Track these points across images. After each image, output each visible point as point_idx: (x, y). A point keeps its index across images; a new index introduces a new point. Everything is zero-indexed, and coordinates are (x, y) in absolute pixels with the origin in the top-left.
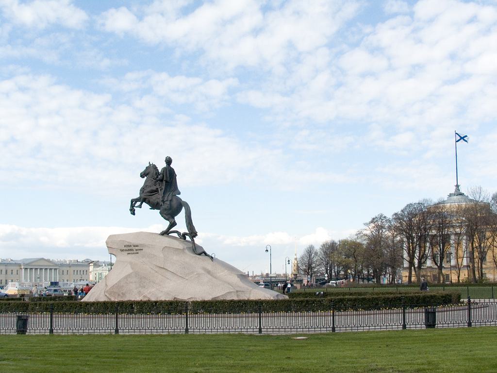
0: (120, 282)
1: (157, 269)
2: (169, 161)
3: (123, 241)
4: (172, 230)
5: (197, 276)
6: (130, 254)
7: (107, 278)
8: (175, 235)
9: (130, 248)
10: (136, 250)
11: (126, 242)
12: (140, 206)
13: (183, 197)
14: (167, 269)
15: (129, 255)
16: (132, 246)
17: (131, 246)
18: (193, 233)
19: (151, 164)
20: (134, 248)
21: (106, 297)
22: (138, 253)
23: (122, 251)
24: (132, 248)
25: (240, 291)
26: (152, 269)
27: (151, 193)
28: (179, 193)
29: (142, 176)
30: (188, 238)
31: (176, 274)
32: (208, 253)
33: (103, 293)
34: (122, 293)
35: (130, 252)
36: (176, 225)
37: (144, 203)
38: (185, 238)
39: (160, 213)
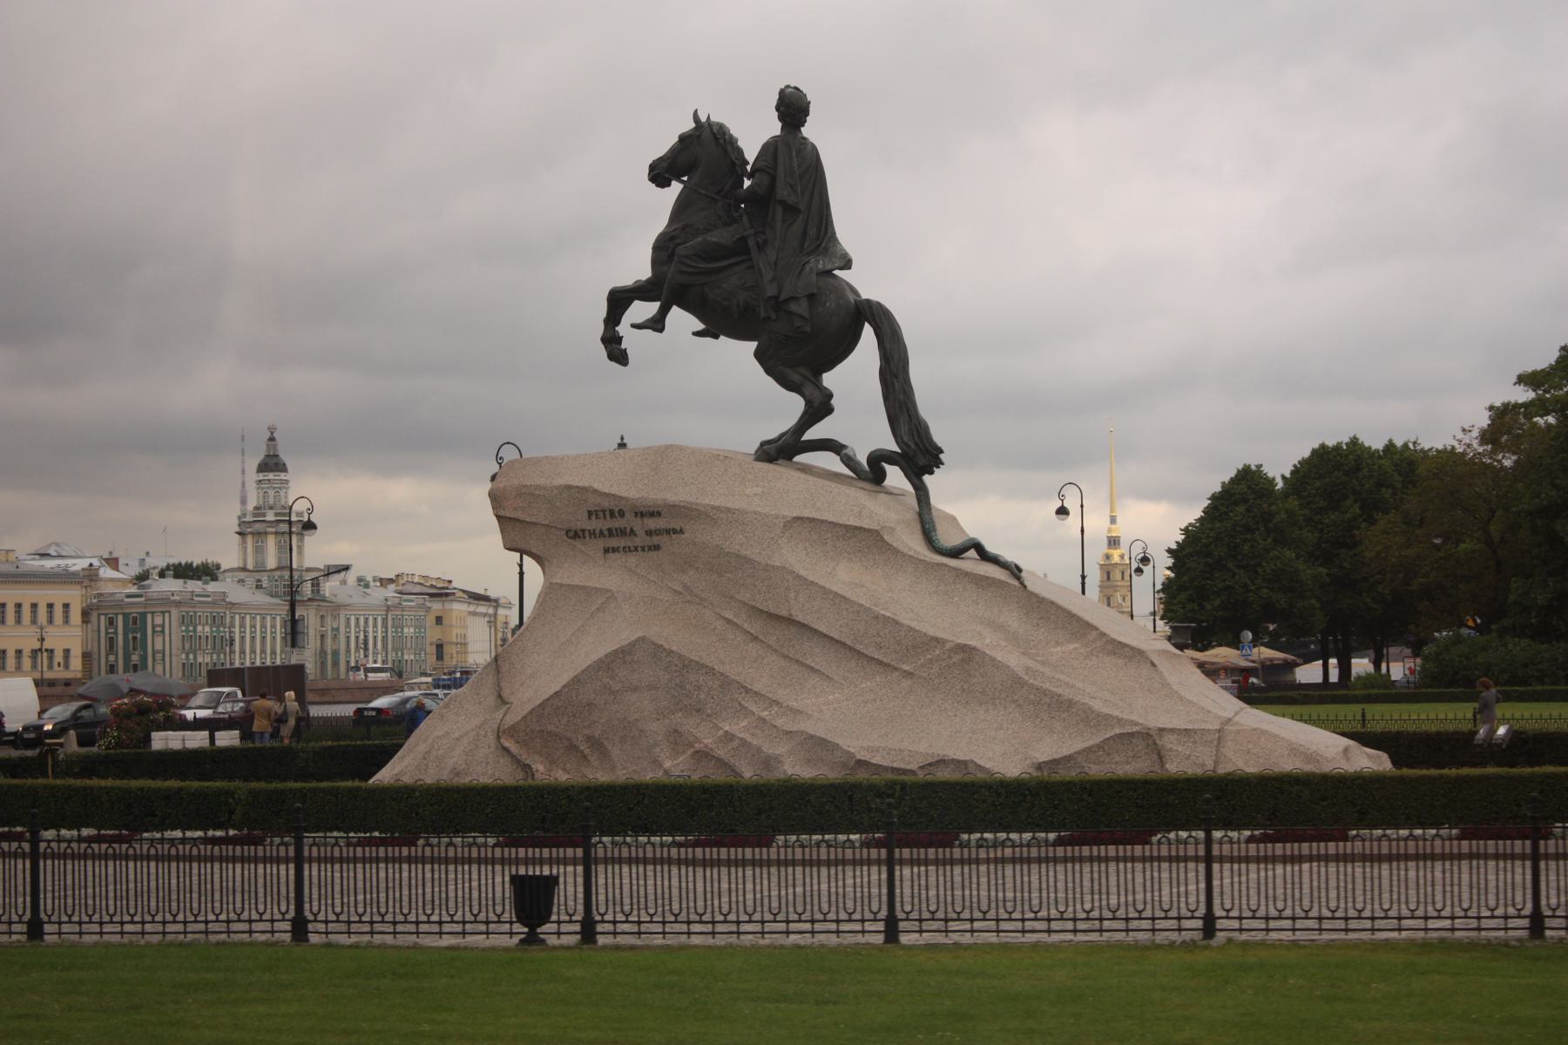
0: (576, 681)
1: (755, 627)
2: (793, 108)
4: (812, 434)
5: (956, 658)
6: (615, 550)
7: (504, 669)
8: (828, 461)
9: (618, 523)
10: (649, 533)
11: (595, 491)
12: (657, 324)
13: (866, 279)
15: (611, 555)
17: (622, 513)
18: (919, 455)
19: (703, 119)
20: (638, 525)
21: (504, 761)
22: (657, 548)
24: (629, 521)
25: (1172, 730)
26: (728, 621)
27: (715, 259)
28: (847, 264)
29: (660, 174)
30: (895, 477)
31: (851, 649)
32: (991, 548)
33: (491, 737)
34: (589, 738)
36: (830, 410)
37: (675, 308)
38: (878, 477)
39: (759, 355)
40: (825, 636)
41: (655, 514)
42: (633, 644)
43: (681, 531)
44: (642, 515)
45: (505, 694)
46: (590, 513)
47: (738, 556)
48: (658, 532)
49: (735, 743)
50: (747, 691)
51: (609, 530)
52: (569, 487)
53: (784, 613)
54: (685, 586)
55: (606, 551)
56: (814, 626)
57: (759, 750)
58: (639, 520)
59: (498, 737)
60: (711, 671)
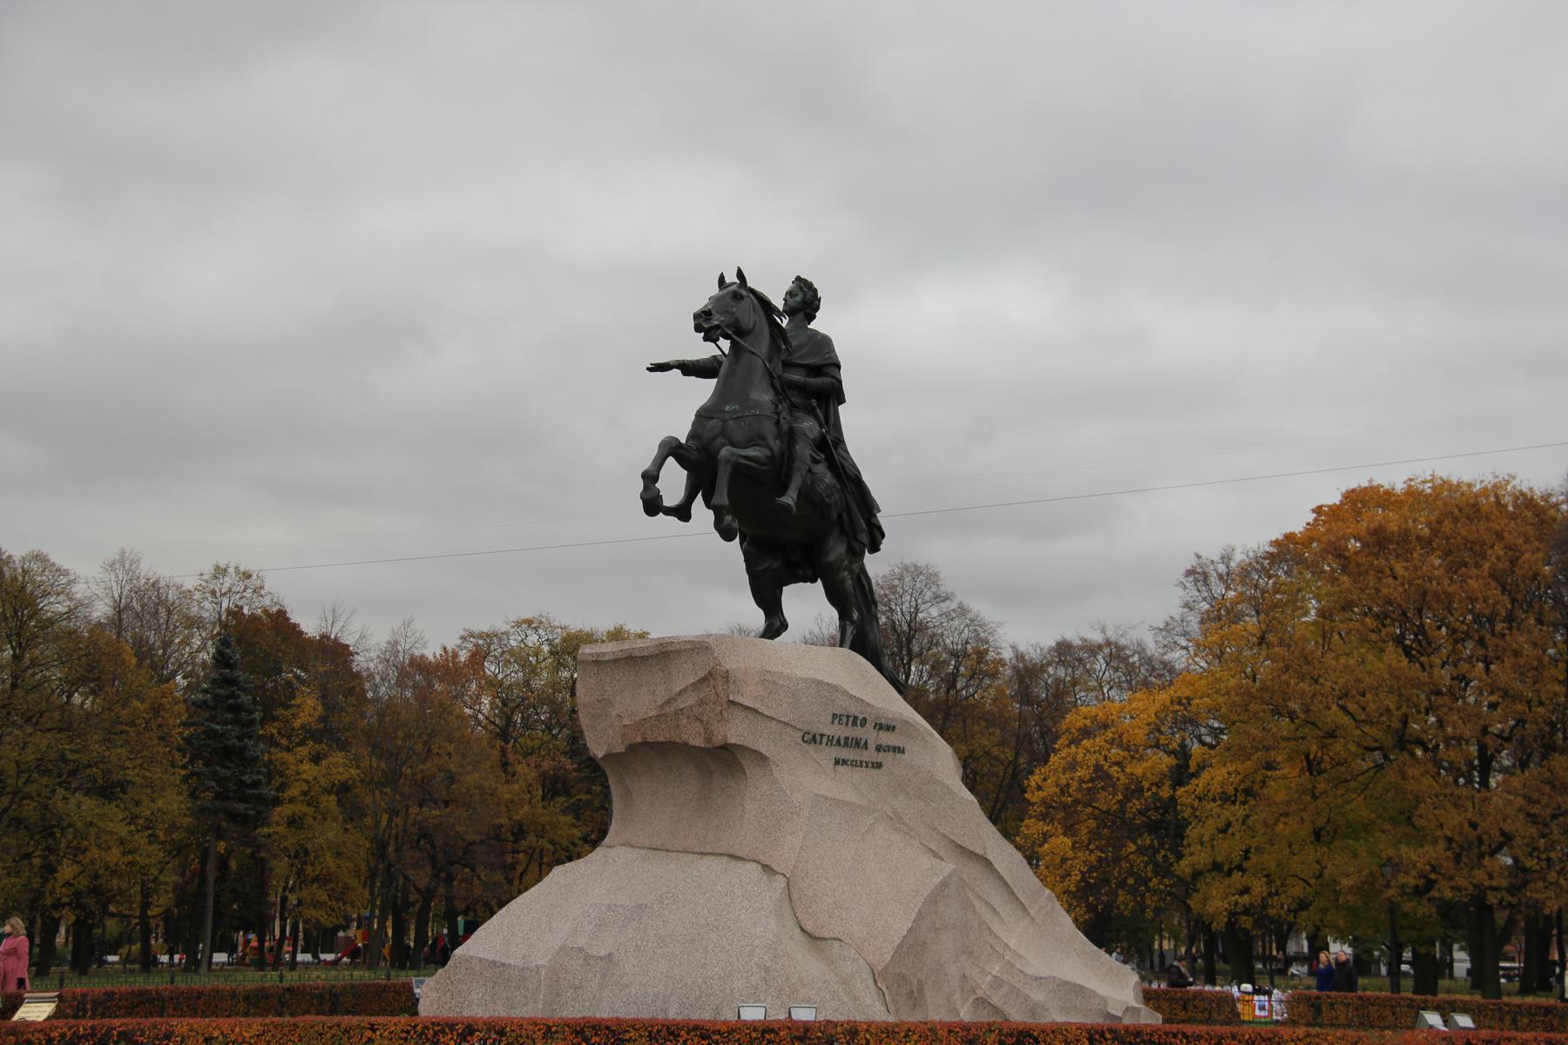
3: (833, 688)
6: (845, 762)
7: (795, 896)
9: (857, 732)
10: (879, 748)
11: (845, 692)
14: (987, 863)
15: (841, 768)
16: (869, 726)
17: (864, 722)
22: (879, 766)
23: (813, 739)
24: (869, 734)
29: (706, 324)
31: (1011, 892)
35: (846, 754)
40: (1001, 878)
41: (890, 728)
42: (950, 876)
43: (901, 751)
44: (880, 727)
45: (809, 928)
46: (835, 716)
47: (943, 785)
49: (1006, 989)
50: (991, 932)
52: (819, 683)
53: (979, 851)
54: (895, 811)
55: (837, 762)
56: (997, 867)
57: (1027, 997)
58: (874, 733)
60: (975, 913)
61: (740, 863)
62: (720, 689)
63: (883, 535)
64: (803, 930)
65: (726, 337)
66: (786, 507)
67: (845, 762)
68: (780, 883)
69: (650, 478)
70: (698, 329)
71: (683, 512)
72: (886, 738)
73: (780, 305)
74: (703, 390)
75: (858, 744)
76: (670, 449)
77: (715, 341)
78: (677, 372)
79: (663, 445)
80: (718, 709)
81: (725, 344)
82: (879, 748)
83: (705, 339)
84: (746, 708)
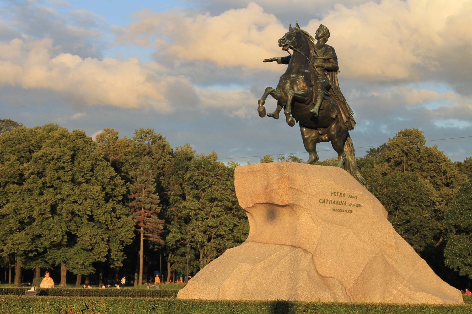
6: (337, 210)
7: (315, 261)
15: (336, 213)
17: (344, 195)
22: (351, 212)
35: (336, 207)
41: (355, 197)
43: (360, 206)
45: (321, 273)
46: (332, 193)
48: (354, 205)
51: (337, 201)
55: (334, 210)
59: (346, 293)
61: (294, 248)
62: (286, 183)
63: (355, 123)
64: (318, 273)
65: (291, 48)
66: (314, 113)
67: (337, 210)
68: (309, 256)
69: (262, 102)
70: (280, 46)
71: (275, 116)
72: (353, 201)
73: (314, 36)
74: (284, 67)
75: (342, 203)
76: (269, 92)
77: (287, 50)
78: (275, 62)
79: (266, 90)
80: (285, 190)
81: (291, 51)
82: (350, 205)
83: (283, 50)
84: (296, 190)
